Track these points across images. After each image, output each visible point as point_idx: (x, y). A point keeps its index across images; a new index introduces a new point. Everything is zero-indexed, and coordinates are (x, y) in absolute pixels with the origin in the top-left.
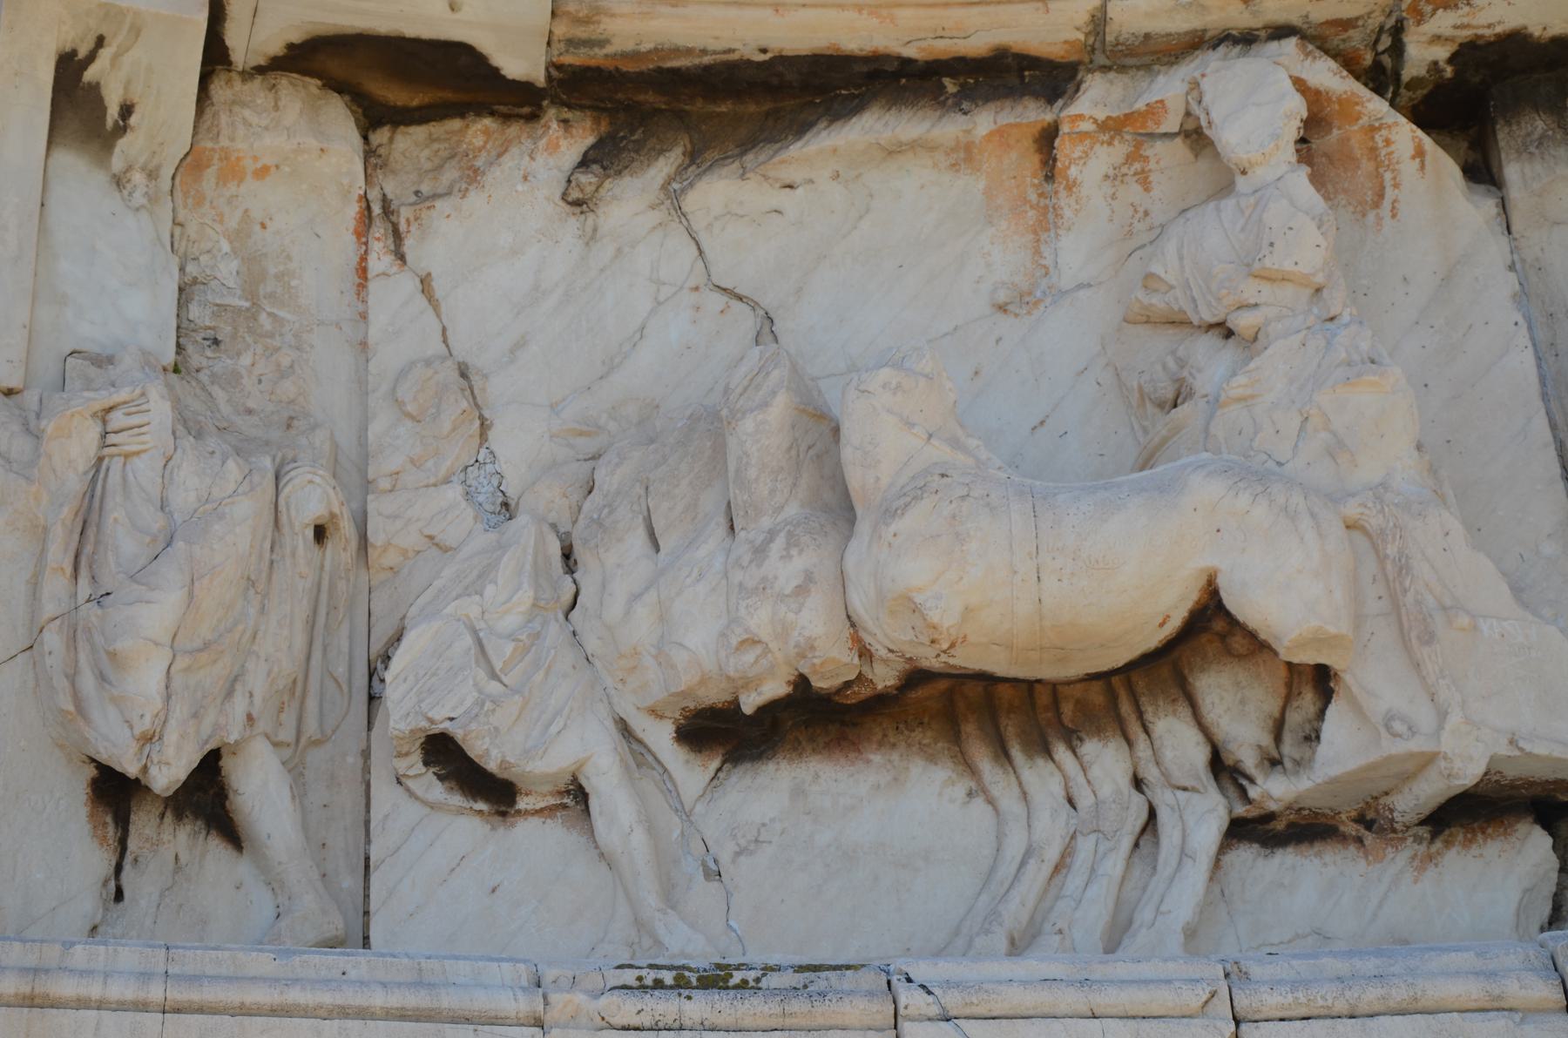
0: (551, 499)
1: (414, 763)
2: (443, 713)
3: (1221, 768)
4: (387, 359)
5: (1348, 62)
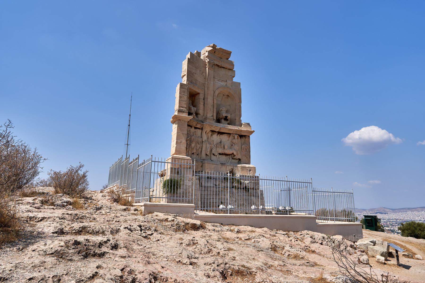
0: (215, 145)
1: (213, 154)
2: (214, 153)
3: (232, 157)
4: (211, 140)
5: (239, 136)
